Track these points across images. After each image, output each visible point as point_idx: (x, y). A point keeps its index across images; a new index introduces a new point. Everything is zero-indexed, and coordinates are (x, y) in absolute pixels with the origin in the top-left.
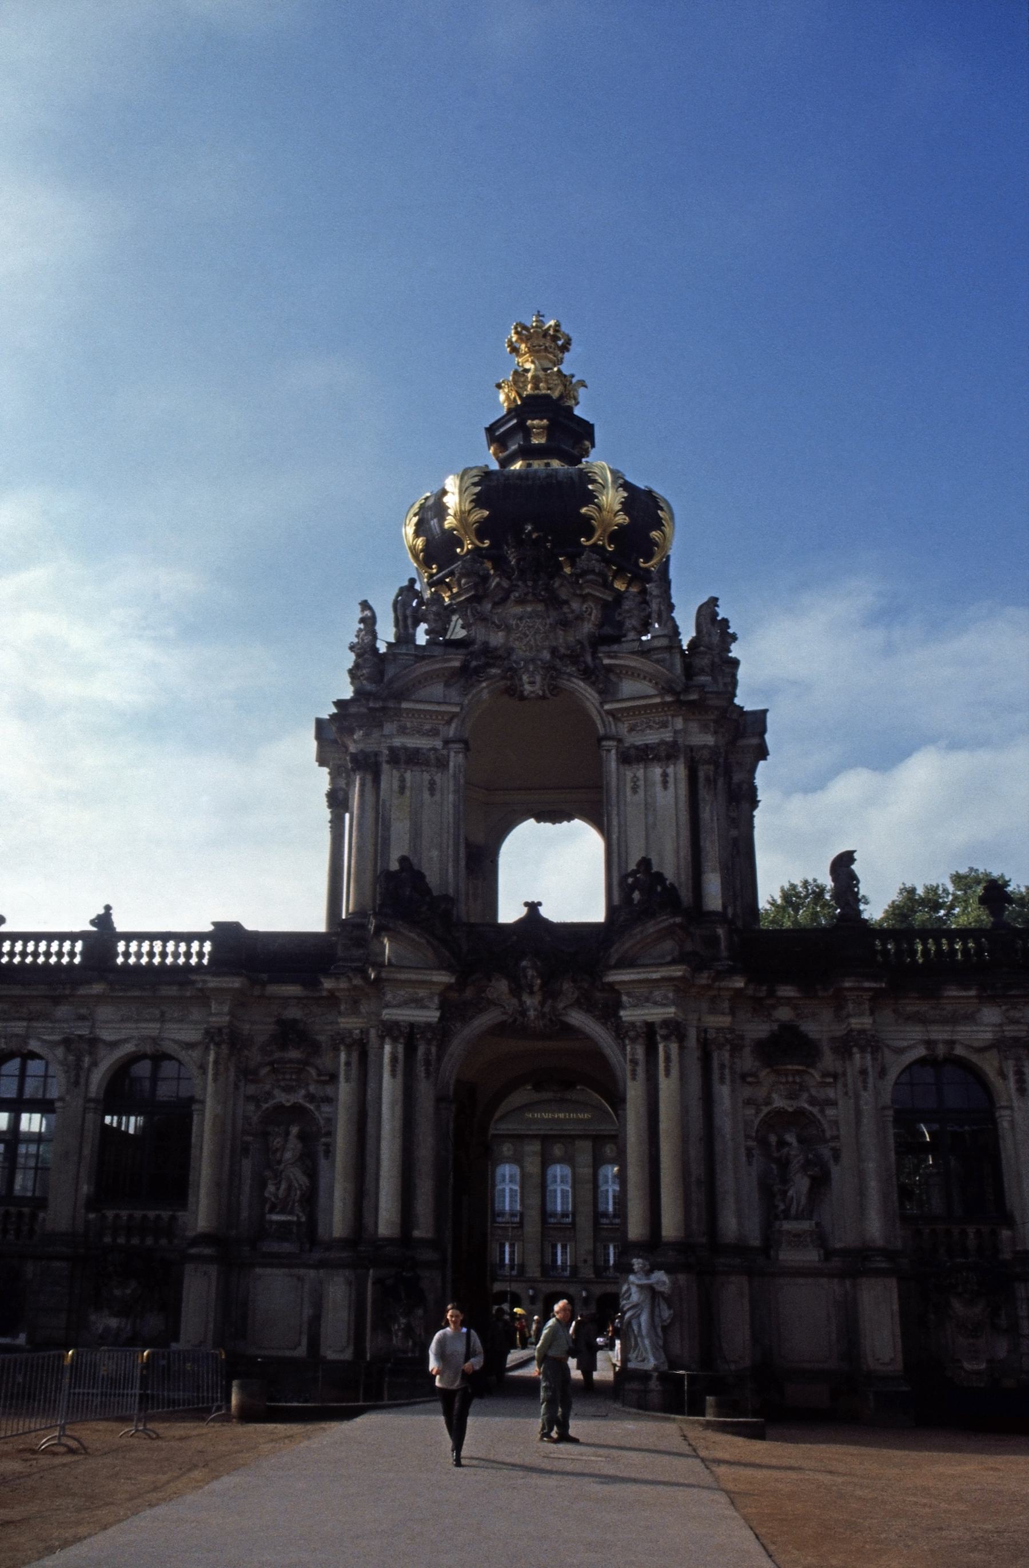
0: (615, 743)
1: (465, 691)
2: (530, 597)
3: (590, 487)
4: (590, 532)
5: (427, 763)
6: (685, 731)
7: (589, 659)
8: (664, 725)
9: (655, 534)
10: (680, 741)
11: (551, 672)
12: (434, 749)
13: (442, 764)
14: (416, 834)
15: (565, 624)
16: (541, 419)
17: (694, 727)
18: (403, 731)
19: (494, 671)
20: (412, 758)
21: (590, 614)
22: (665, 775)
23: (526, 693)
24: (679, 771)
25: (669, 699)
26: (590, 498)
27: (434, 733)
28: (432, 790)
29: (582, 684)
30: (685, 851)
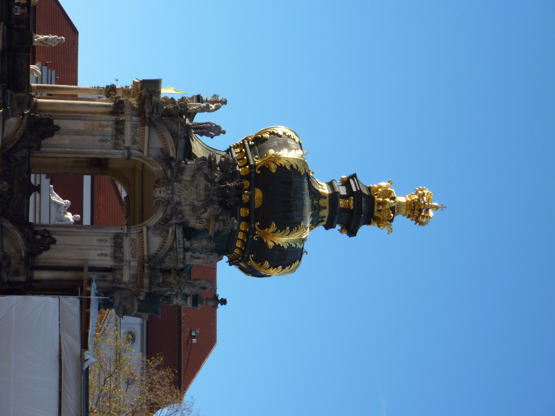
0: (125, 232)
1: (158, 159)
2: (208, 193)
3: (288, 228)
4: (262, 227)
5: (117, 139)
6: (130, 266)
7: (174, 221)
8: (134, 256)
9: (267, 264)
10: (125, 263)
11: (168, 202)
12: (124, 142)
13: (116, 146)
14: (78, 133)
15: (194, 208)
16: (354, 205)
17: (134, 271)
18: (134, 127)
19: (169, 173)
20: (119, 130)
21: (200, 223)
22: (106, 255)
23: (156, 189)
24: (108, 262)
25: (146, 258)
26: (281, 228)
27: (134, 142)
28: (102, 141)
29: (160, 217)
30: (65, 263)
